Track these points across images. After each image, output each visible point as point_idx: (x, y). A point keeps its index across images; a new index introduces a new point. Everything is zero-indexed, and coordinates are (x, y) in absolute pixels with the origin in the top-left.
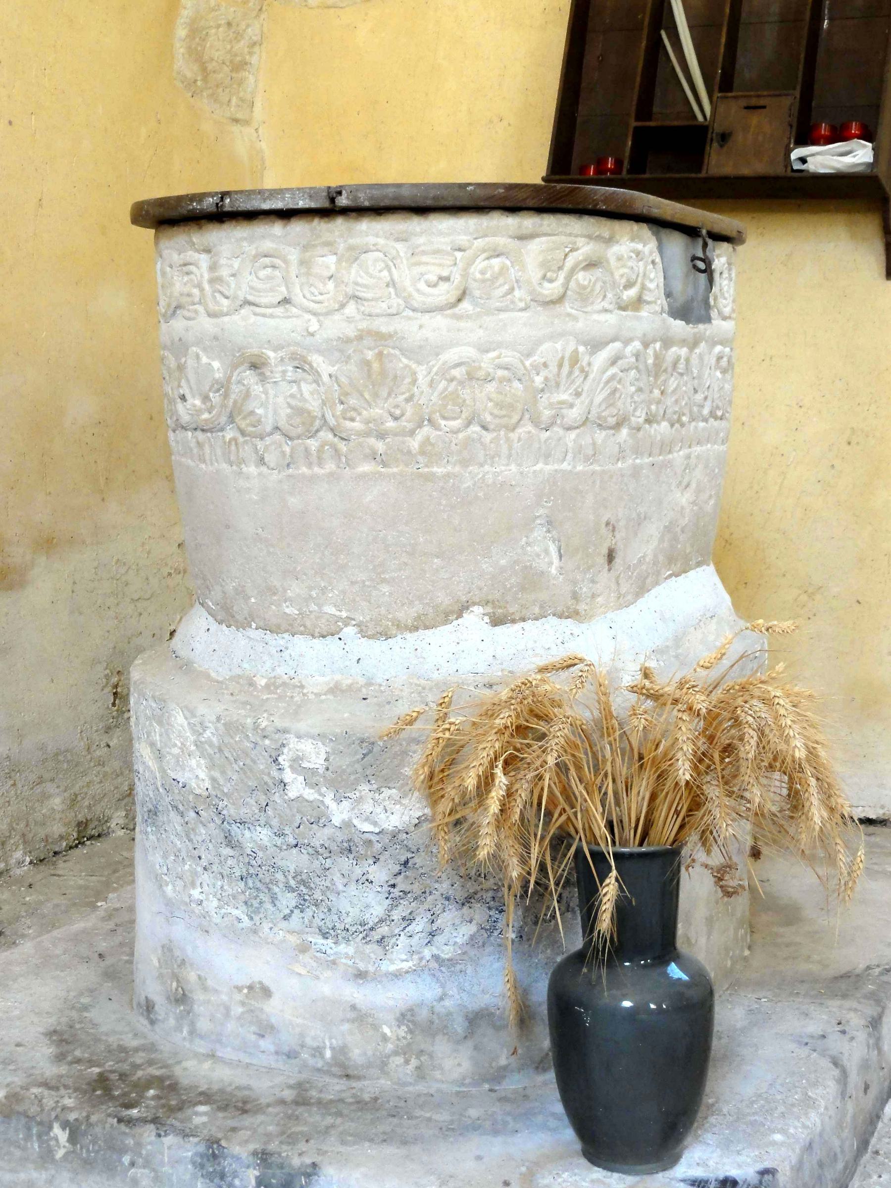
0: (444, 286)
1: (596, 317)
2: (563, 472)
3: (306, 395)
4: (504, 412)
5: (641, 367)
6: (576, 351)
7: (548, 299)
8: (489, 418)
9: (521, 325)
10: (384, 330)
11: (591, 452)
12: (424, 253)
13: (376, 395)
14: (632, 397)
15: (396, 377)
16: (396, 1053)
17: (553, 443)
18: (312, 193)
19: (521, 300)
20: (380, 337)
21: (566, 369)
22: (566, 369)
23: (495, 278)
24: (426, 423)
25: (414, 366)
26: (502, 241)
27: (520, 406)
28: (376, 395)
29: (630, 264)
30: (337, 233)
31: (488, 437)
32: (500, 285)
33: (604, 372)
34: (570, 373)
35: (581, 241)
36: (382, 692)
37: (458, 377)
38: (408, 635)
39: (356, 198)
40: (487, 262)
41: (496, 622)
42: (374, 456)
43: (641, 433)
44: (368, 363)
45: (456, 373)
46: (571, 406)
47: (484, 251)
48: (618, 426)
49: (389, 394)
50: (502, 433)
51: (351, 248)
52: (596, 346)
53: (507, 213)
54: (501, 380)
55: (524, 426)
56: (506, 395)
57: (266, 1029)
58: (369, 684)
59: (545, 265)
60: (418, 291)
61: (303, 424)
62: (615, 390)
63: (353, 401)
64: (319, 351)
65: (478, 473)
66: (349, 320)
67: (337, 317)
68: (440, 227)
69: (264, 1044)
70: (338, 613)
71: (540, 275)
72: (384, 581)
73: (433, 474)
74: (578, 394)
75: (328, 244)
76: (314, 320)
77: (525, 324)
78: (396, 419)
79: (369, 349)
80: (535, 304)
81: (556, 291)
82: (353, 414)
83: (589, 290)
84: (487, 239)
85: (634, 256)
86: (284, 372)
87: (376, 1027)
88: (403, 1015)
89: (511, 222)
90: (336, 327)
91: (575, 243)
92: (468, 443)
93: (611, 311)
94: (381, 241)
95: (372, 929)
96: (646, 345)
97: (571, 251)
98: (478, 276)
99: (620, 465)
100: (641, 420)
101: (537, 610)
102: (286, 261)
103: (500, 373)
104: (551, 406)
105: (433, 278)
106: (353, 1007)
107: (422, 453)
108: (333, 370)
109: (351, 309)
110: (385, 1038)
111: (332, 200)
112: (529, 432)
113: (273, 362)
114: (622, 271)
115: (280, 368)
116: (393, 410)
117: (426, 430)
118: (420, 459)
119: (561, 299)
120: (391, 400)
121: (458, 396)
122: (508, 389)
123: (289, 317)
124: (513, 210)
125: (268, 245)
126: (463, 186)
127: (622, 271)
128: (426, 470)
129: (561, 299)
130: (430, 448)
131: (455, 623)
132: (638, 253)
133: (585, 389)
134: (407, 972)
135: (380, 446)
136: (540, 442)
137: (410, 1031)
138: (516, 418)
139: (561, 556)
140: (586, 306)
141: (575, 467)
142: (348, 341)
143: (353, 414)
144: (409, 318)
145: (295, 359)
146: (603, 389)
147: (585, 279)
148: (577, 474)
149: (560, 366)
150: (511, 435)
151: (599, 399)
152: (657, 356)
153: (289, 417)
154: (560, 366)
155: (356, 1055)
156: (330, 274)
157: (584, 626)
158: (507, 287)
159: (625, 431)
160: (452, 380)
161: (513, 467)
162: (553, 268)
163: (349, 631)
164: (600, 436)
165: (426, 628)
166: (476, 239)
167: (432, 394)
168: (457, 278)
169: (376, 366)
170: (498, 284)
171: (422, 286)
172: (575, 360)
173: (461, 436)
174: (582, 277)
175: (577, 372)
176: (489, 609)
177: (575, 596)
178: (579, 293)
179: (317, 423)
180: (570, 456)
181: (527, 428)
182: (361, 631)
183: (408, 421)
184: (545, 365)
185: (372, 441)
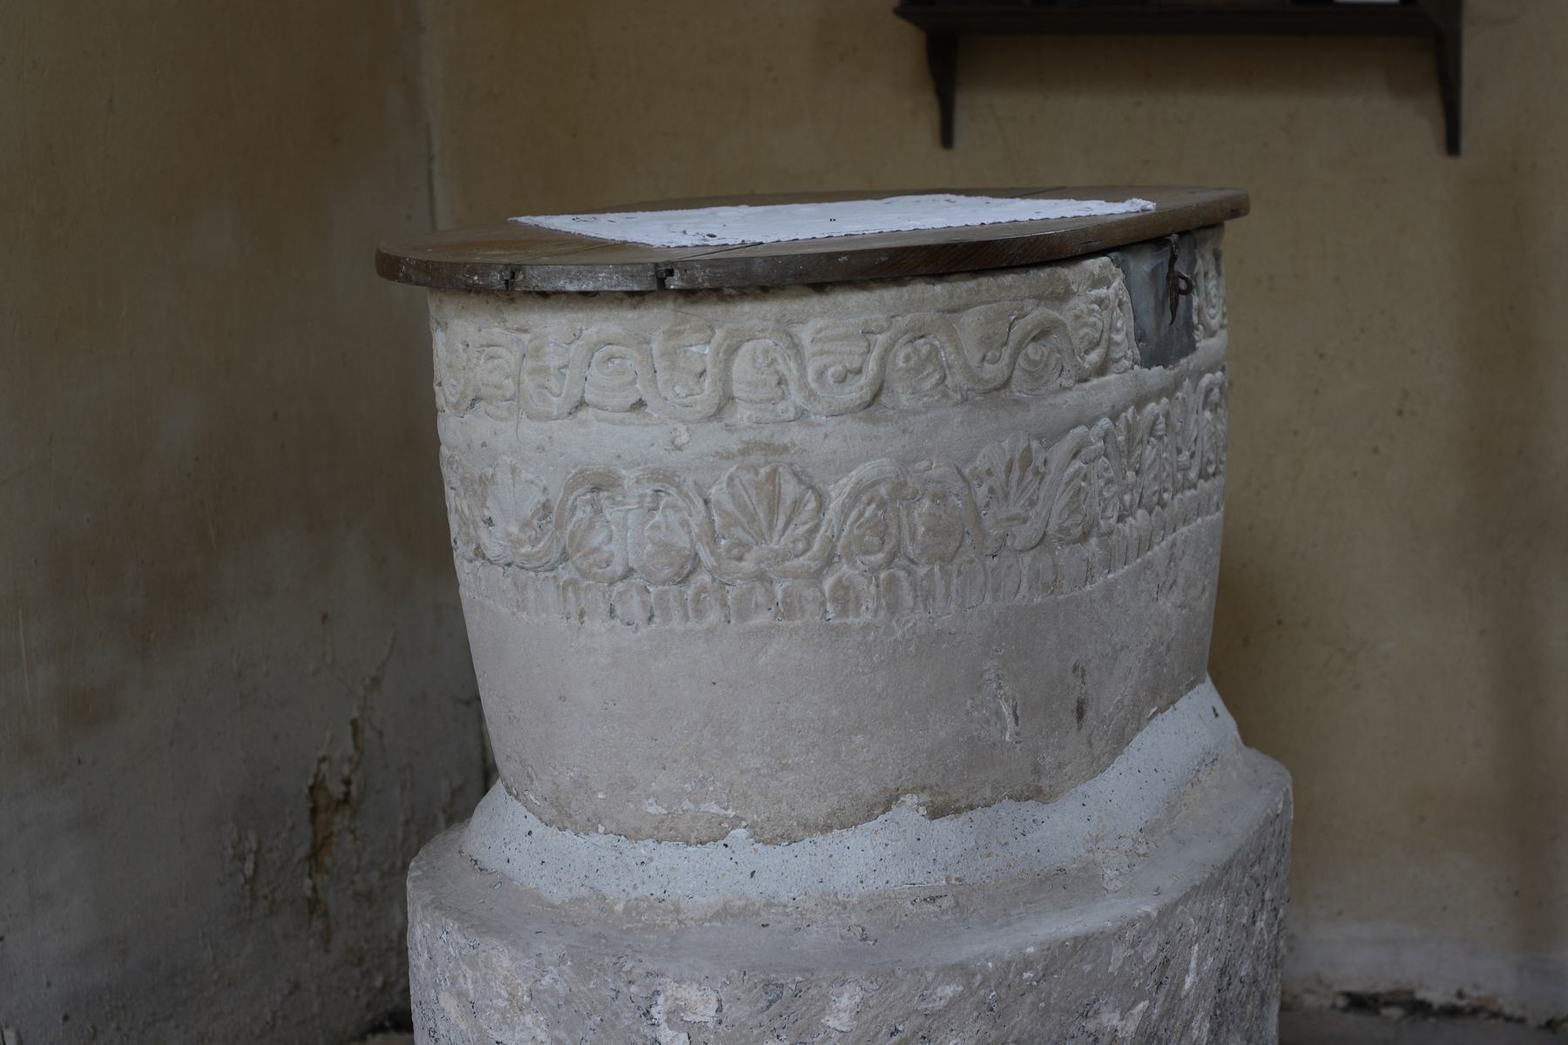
5: (1110, 449)
6: (1028, 449)
11: (1050, 577)
14: (1101, 494)
21: (1016, 474)
22: (1016, 474)
29: (1092, 319)
34: (1021, 479)
35: (1029, 305)
36: (788, 915)
38: (819, 838)
41: (936, 813)
43: (1114, 537)
46: (1025, 520)
48: (1085, 537)
52: (1050, 437)
58: (769, 905)
59: (986, 342)
62: (1080, 489)
70: (723, 812)
71: (979, 356)
72: (784, 767)
73: (848, 627)
74: (1033, 503)
76: (682, 428)
85: (1096, 307)
93: (1070, 389)
96: (1114, 418)
99: (1088, 588)
100: (1113, 521)
101: (988, 793)
114: (1082, 332)
120: (789, 532)
127: (1082, 332)
128: (838, 621)
131: (881, 818)
132: (1100, 302)
133: (1042, 495)
145: (657, 480)
149: (1009, 470)
152: (1129, 428)
154: (1009, 470)
157: (1047, 808)
159: (1093, 541)
163: (740, 833)
164: (1062, 553)
165: (843, 826)
168: (872, 367)
175: (1029, 476)
176: (925, 797)
177: (1037, 770)
180: (1024, 585)
184: (989, 472)
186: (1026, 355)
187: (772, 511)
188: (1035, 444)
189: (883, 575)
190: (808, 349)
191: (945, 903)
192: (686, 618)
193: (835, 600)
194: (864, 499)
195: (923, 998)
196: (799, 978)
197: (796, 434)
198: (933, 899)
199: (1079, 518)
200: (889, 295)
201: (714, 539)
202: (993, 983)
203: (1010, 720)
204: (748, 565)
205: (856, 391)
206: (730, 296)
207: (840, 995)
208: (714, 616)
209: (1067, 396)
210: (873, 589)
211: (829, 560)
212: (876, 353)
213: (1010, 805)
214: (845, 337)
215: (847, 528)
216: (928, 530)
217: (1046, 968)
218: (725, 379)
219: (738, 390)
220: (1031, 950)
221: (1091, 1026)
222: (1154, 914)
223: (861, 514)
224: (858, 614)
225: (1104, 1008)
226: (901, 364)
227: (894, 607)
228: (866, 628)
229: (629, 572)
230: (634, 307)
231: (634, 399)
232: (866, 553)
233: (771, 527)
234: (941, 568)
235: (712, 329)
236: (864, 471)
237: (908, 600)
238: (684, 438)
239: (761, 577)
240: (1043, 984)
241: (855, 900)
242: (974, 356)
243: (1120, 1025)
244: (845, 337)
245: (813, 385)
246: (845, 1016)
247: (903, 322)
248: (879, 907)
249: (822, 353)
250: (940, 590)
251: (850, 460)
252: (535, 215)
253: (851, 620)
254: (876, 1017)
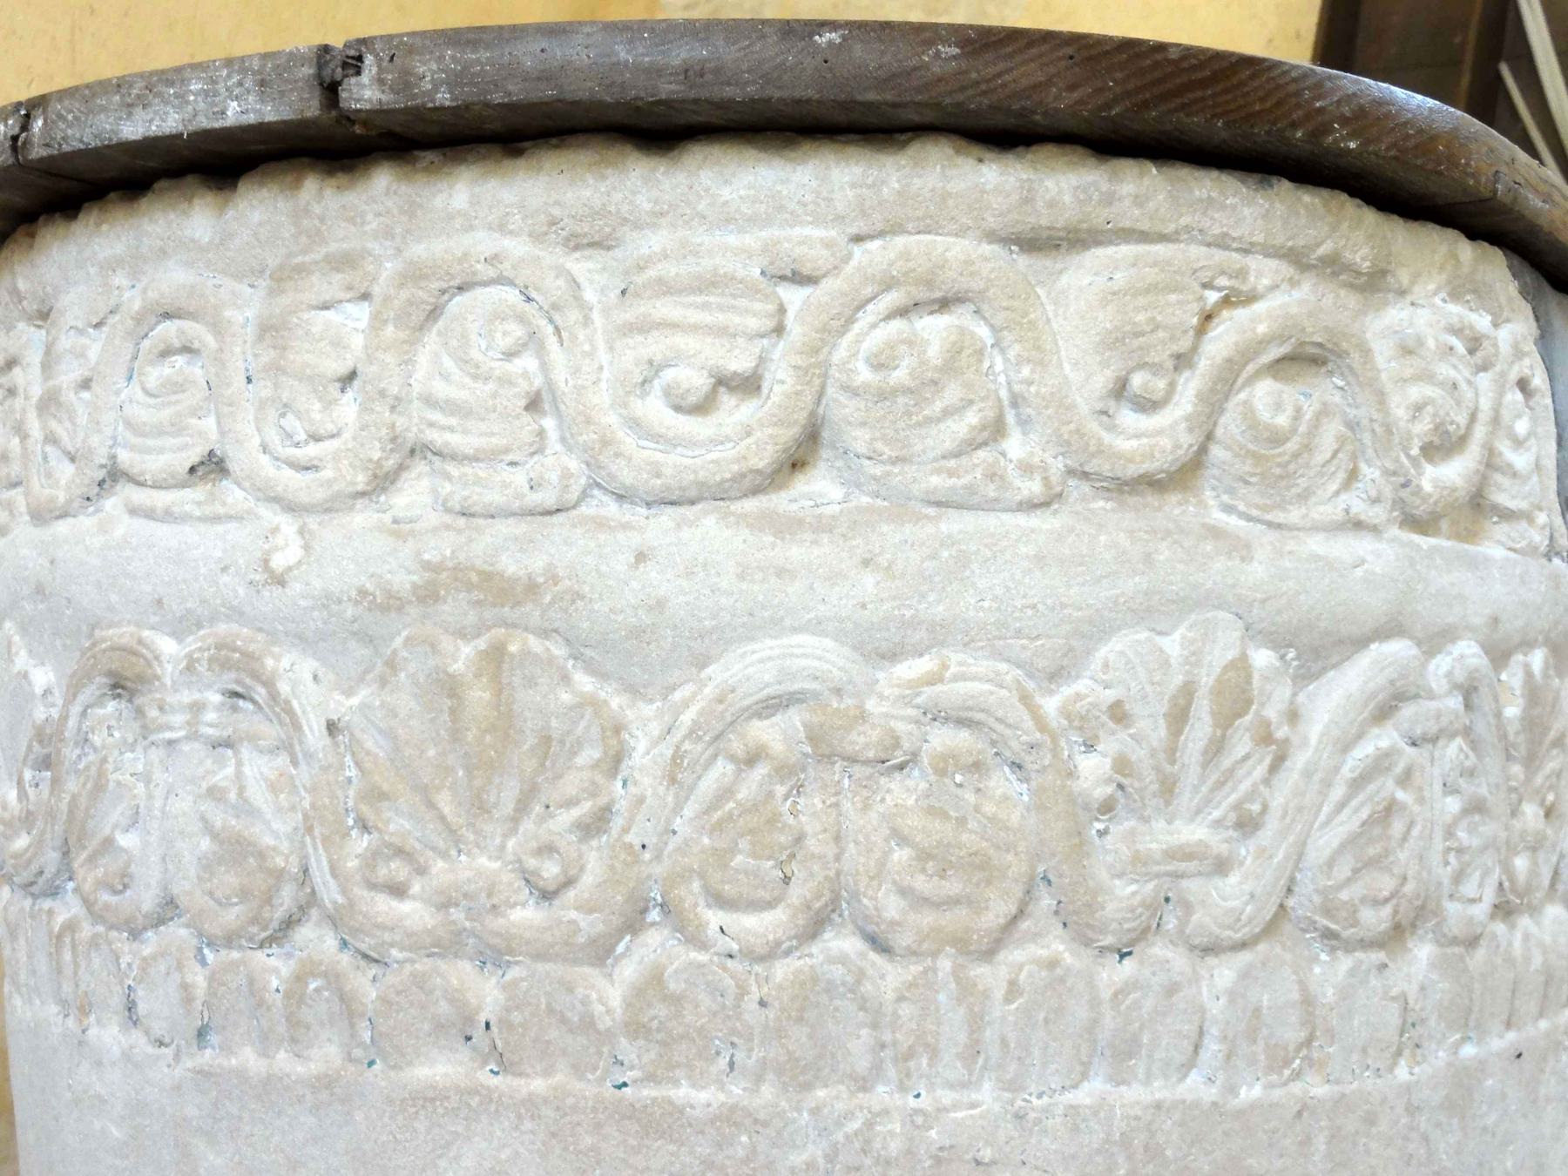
0: (735, 413)
1: (1316, 544)
2: (1189, 1109)
3: (258, 795)
4: (953, 886)
5: (1481, 728)
6: (1241, 665)
7: (1132, 471)
8: (892, 907)
9: (1024, 561)
10: (510, 565)
11: (1293, 1034)
12: (664, 288)
13: (480, 807)
14: (1449, 833)
15: (546, 740)
17: (1148, 1004)
18: (267, 72)
19: (1026, 469)
20: (499, 592)
21: (1200, 729)
22: (1200, 729)
23: (926, 385)
24: (654, 915)
25: (615, 702)
26: (957, 252)
27: (1017, 867)
28: (480, 807)
29: (1445, 370)
30: (373, 224)
31: (890, 977)
32: (947, 413)
33: (1346, 747)
34: (1216, 748)
35: (1264, 272)
37: (777, 747)
39: (405, 82)
40: (897, 325)
42: (461, 1028)
43: (1481, 953)
44: (451, 687)
45: (770, 733)
46: (1222, 866)
47: (888, 285)
48: (1397, 935)
49: (522, 807)
50: (945, 964)
51: (414, 275)
52: (1316, 649)
53: (977, 150)
54: (945, 765)
55: (1035, 937)
56: (962, 821)
60: (635, 424)
61: (244, 894)
62: (1390, 809)
63: (398, 824)
64: (303, 641)
65: (849, 1115)
66: (400, 530)
67: (362, 518)
68: (726, 193)
71: (1102, 380)
73: (676, 1111)
74: (1247, 824)
75: (344, 262)
76: (288, 526)
77: (1040, 560)
78: (547, 896)
79: (462, 634)
80: (1086, 487)
81: (1166, 442)
82: (397, 869)
83: (1291, 446)
84: (900, 241)
85: (1460, 348)
86: (197, 708)
90: (362, 551)
91: (1241, 274)
92: (809, 997)
93: (1375, 530)
94: (517, 247)
96: (1499, 655)
97: (1226, 302)
98: (864, 375)
99: (1402, 1073)
100: (1480, 911)
102: (217, 328)
103: (942, 738)
104: (1139, 864)
105: (695, 380)
107: (636, 1028)
108: (344, 706)
109: (414, 495)
111: (331, 90)
112: (1053, 964)
113: (168, 672)
114: (1416, 392)
115: (186, 697)
116: (531, 863)
117: (655, 943)
118: (627, 1049)
119: (1183, 475)
120: (528, 825)
121: (773, 820)
122: (971, 797)
123: (216, 519)
124: (1002, 133)
125: (173, 278)
126: (798, 31)
127: (1416, 392)
128: (649, 1092)
129: (1183, 475)
130: (661, 1010)
132: (1475, 343)
133: (1277, 801)
135: (487, 993)
136: (1095, 1003)
138: (999, 909)
140: (1281, 506)
141: (1232, 1090)
142: (389, 603)
143: (397, 869)
144: (601, 524)
145: (226, 665)
146: (1341, 805)
147: (1278, 407)
148: (1240, 1114)
149: (1179, 717)
150: (981, 972)
151: (1325, 842)
152: (1534, 694)
153: (208, 866)
154: (1179, 717)
156: (343, 370)
158: (972, 418)
159: (1423, 952)
160: (752, 759)
161: (987, 1095)
162: (1153, 357)
164: (1330, 972)
166: (858, 239)
167: (677, 809)
168: (781, 380)
169: (478, 695)
170: (938, 406)
171: (654, 409)
172: (1236, 696)
173: (782, 970)
174: (1265, 397)
175: (1241, 744)
178: (1258, 458)
179: (287, 897)
180: (1212, 1047)
181: (1046, 945)
183: (587, 908)
184: (1119, 714)
185: (461, 973)
186: (1248, 411)
199: (1386, 884)
229: (169, 908)
231: (194, 456)
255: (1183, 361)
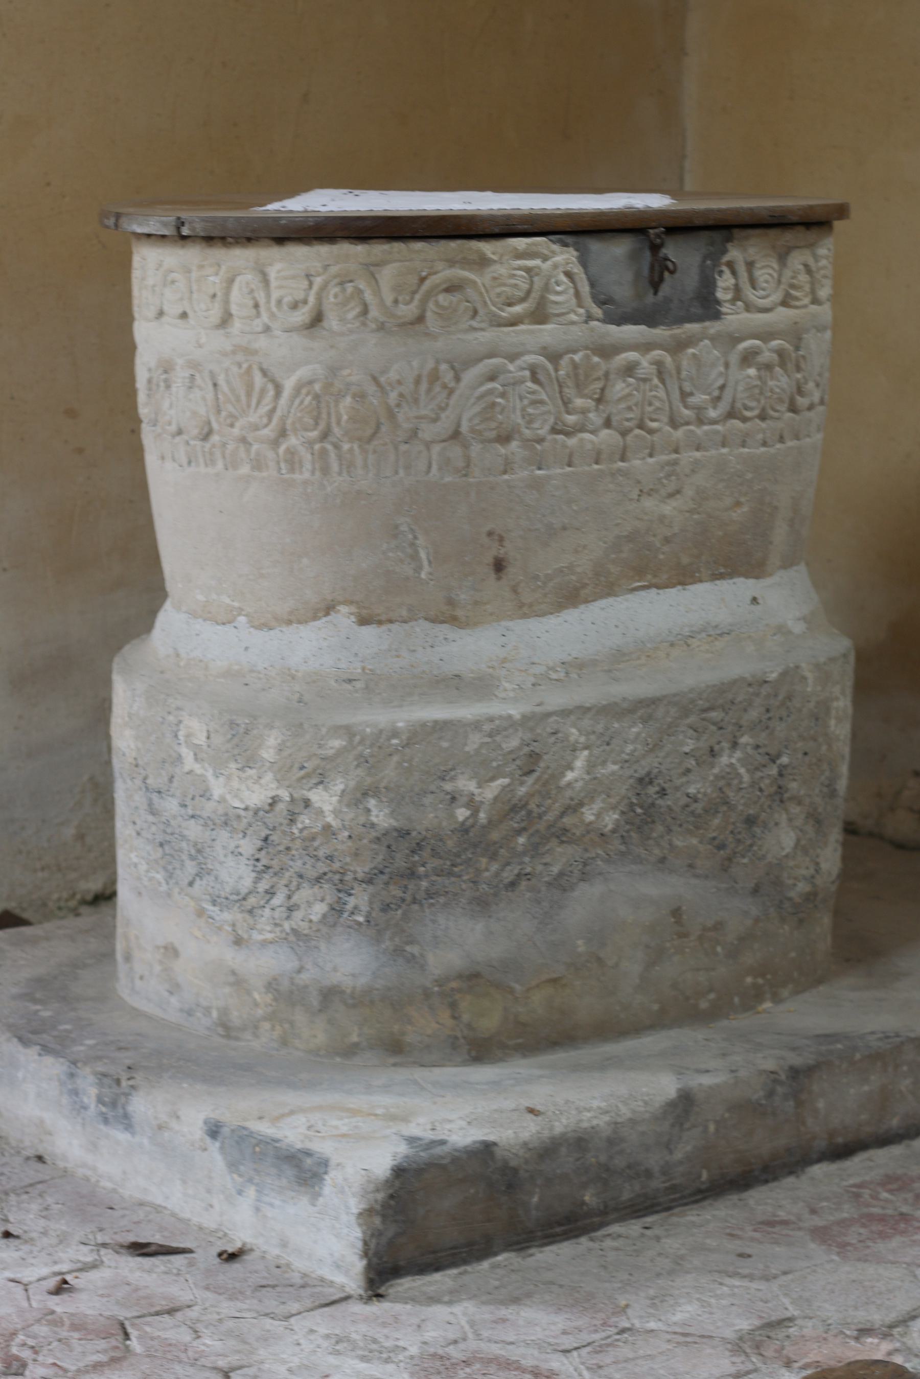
11: (461, 464)
16: (265, 1019)
21: (424, 386)
22: (424, 386)
34: (429, 390)
35: (440, 265)
36: (260, 679)
38: (284, 629)
41: (363, 621)
57: (175, 988)
58: (252, 671)
59: (397, 288)
62: (493, 405)
69: (174, 1000)
87: (249, 993)
88: (270, 984)
89: (359, 250)
95: (244, 899)
101: (404, 613)
106: (233, 973)
110: (256, 1005)
119: (421, 319)
127: (498, 290)
128: (287, 476)
131: (324, 619)
134: (271, 943)
137: (275, 999)
138: (369, 432)
139: (430, 562)
149: (418, 381)
155: (236, 1018)
157: (462, 632)
163: (242, 619)
165: (300, 622)
168: (312, 299)
172: (434, 376)
174: (442, 299)
175: (437, 388)
177: (451, 602)
180: (435, 467)
182: (250, 622)
184: (399, 382)
186: (437, 304)
187: (249, 394)
188: (444, 367)
189: (317, 447)
190: (274, 284)
191: (359, 685)
192: (206, 465)
193: (286, 461)
194: (304, 391)
195: (320, 746)
196: (247, 721)
197: (262, 343)
198: (350, 681)
199: (493, 425)
200: (324, 250)
201: (219, 411)
202: (368, 742)
203: (425, 563)
204: (236, 431)
205: (302, 316)
206: (230, 243)
207: (269, 736)
208: (245, 469)
209: (479, 335)
210: (309, 457)
211: (283, 433)
212: (315, 288)
213: (427, 625)
214: (294, 277)
215: (293, 411)
216: (350, 418)
217: (409, 739)
218: (226, 302)
219: (234, 309)
220: (400, 724)
221: (448, 787)
222: (518, 717)
223: (302, 402)
224: (301, 473)
225: (460, 776)
226: (332, 299)
227: (325, 470)
228: (306, 483)
230: (183, 247)
232: (306, 430)
233: (249, 406)
234: (360, 447)
235: (219, 266)
236: (303, 372)
237: (335, 466)
238: (203, 340)
239: (243, 440)
240: (407, 750)
241: (300, 674)
242: (389, 298)
243: (476, 791)
244: (294, 277)
245: (274, 309)
246: (272, 751)
247: (334, 270)
248: (314, 682)
249: (280, 287)
250: (359, 461)
251: (297, 361)
252: (292, 192)
253: (297, 476)
254: (290, 755)
255: (414, 292)
